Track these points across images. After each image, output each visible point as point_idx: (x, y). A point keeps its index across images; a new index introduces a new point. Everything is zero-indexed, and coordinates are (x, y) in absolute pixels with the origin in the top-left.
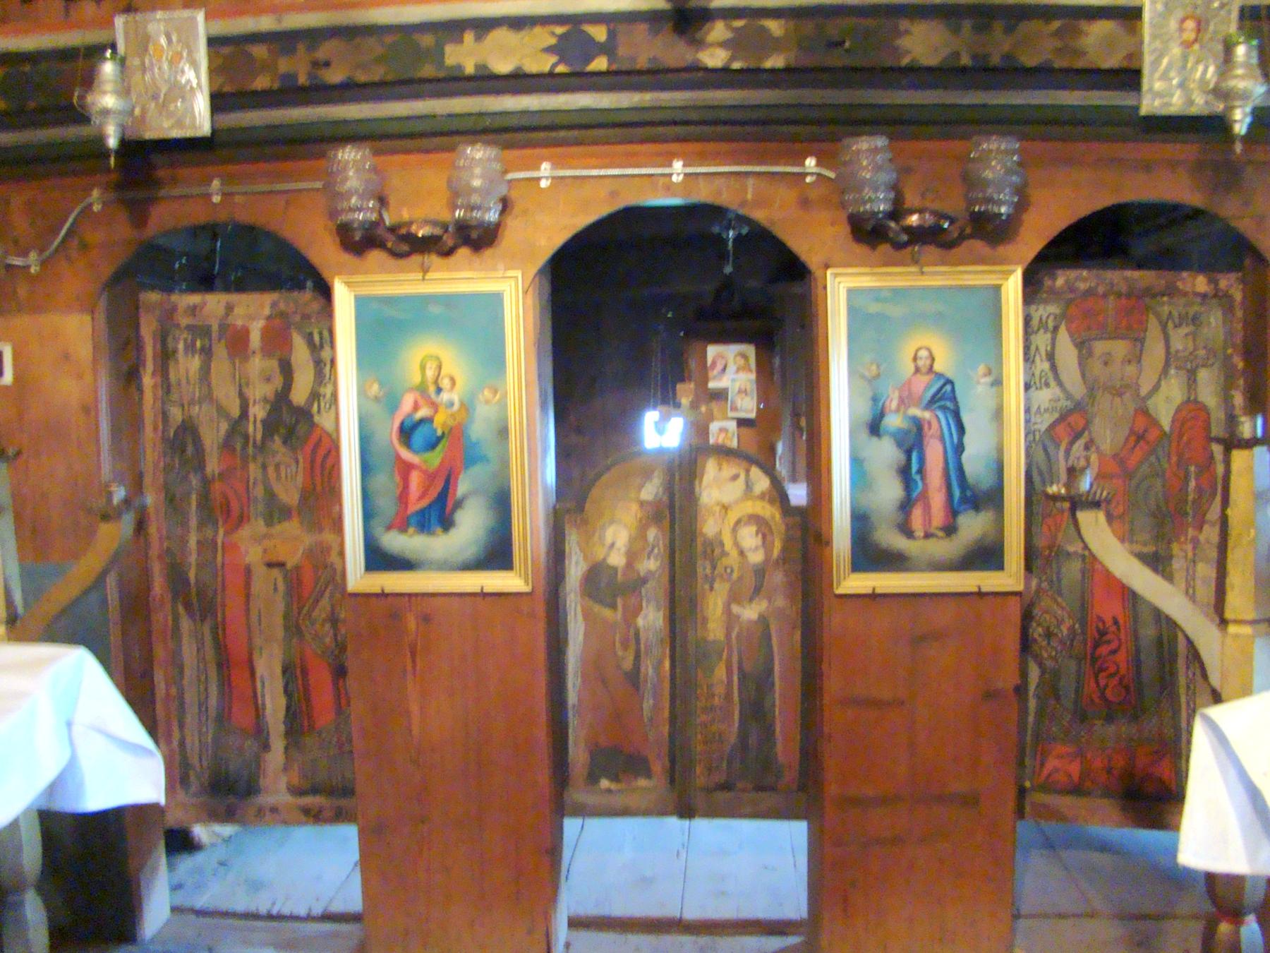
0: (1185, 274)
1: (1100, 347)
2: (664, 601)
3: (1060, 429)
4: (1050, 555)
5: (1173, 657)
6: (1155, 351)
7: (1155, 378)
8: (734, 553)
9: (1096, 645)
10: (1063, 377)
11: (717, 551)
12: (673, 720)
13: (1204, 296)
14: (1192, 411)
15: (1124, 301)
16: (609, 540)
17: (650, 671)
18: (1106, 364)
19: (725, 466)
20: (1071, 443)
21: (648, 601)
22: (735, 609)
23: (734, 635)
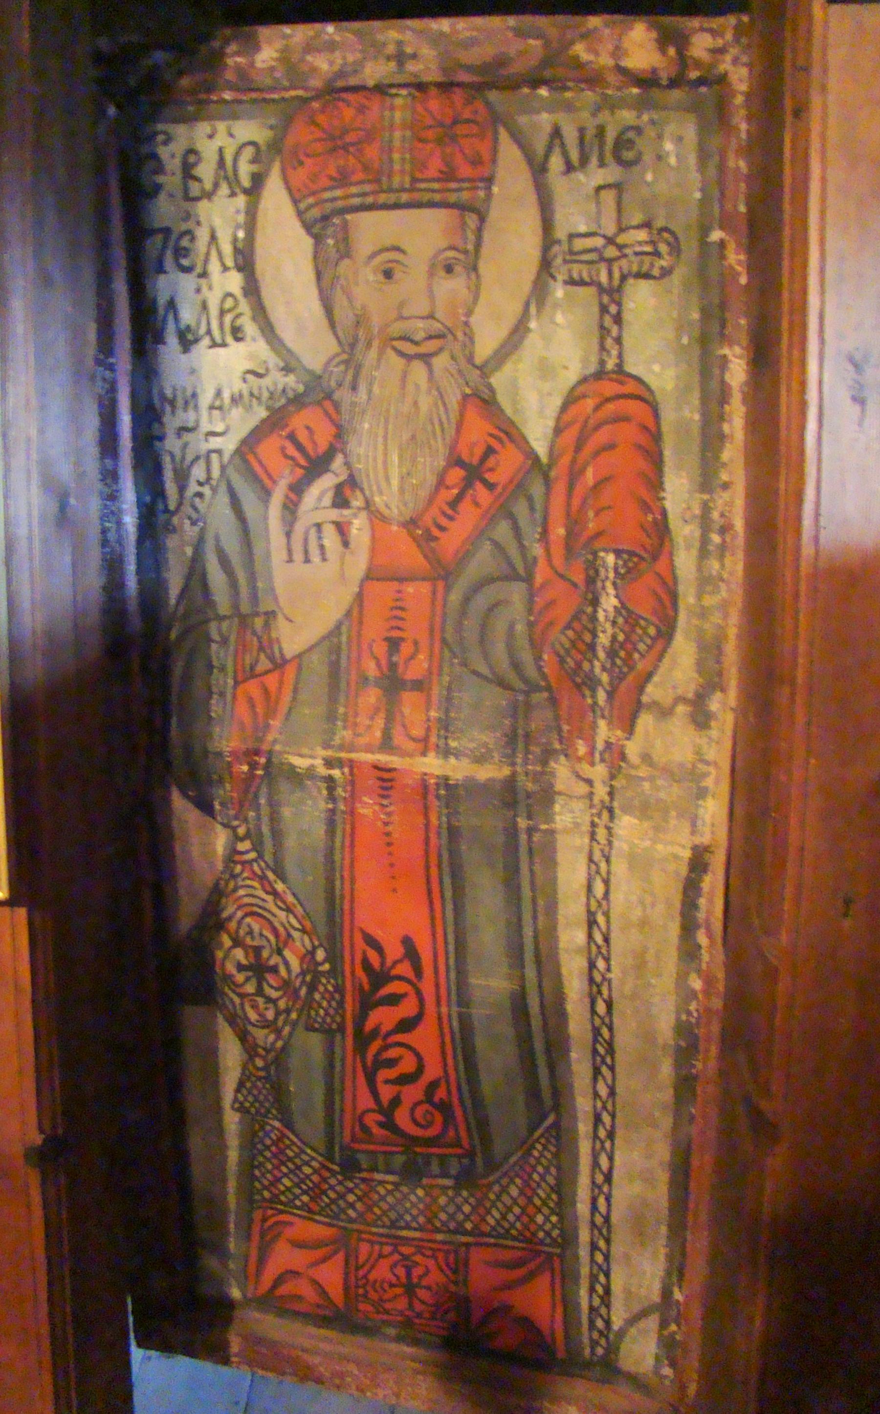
0: (594, 21)
1: (372, 229)
3: (270, 450)
4: (251, 775)
5: (557, 1045)
6: (514, 237)
7: (513, 309)
9: (366, 1005)
10: (278, 312)
13: (647, 81)
14: (611, 398)
15: (435, 104)
18: (388, 274)
20: (297, 489)
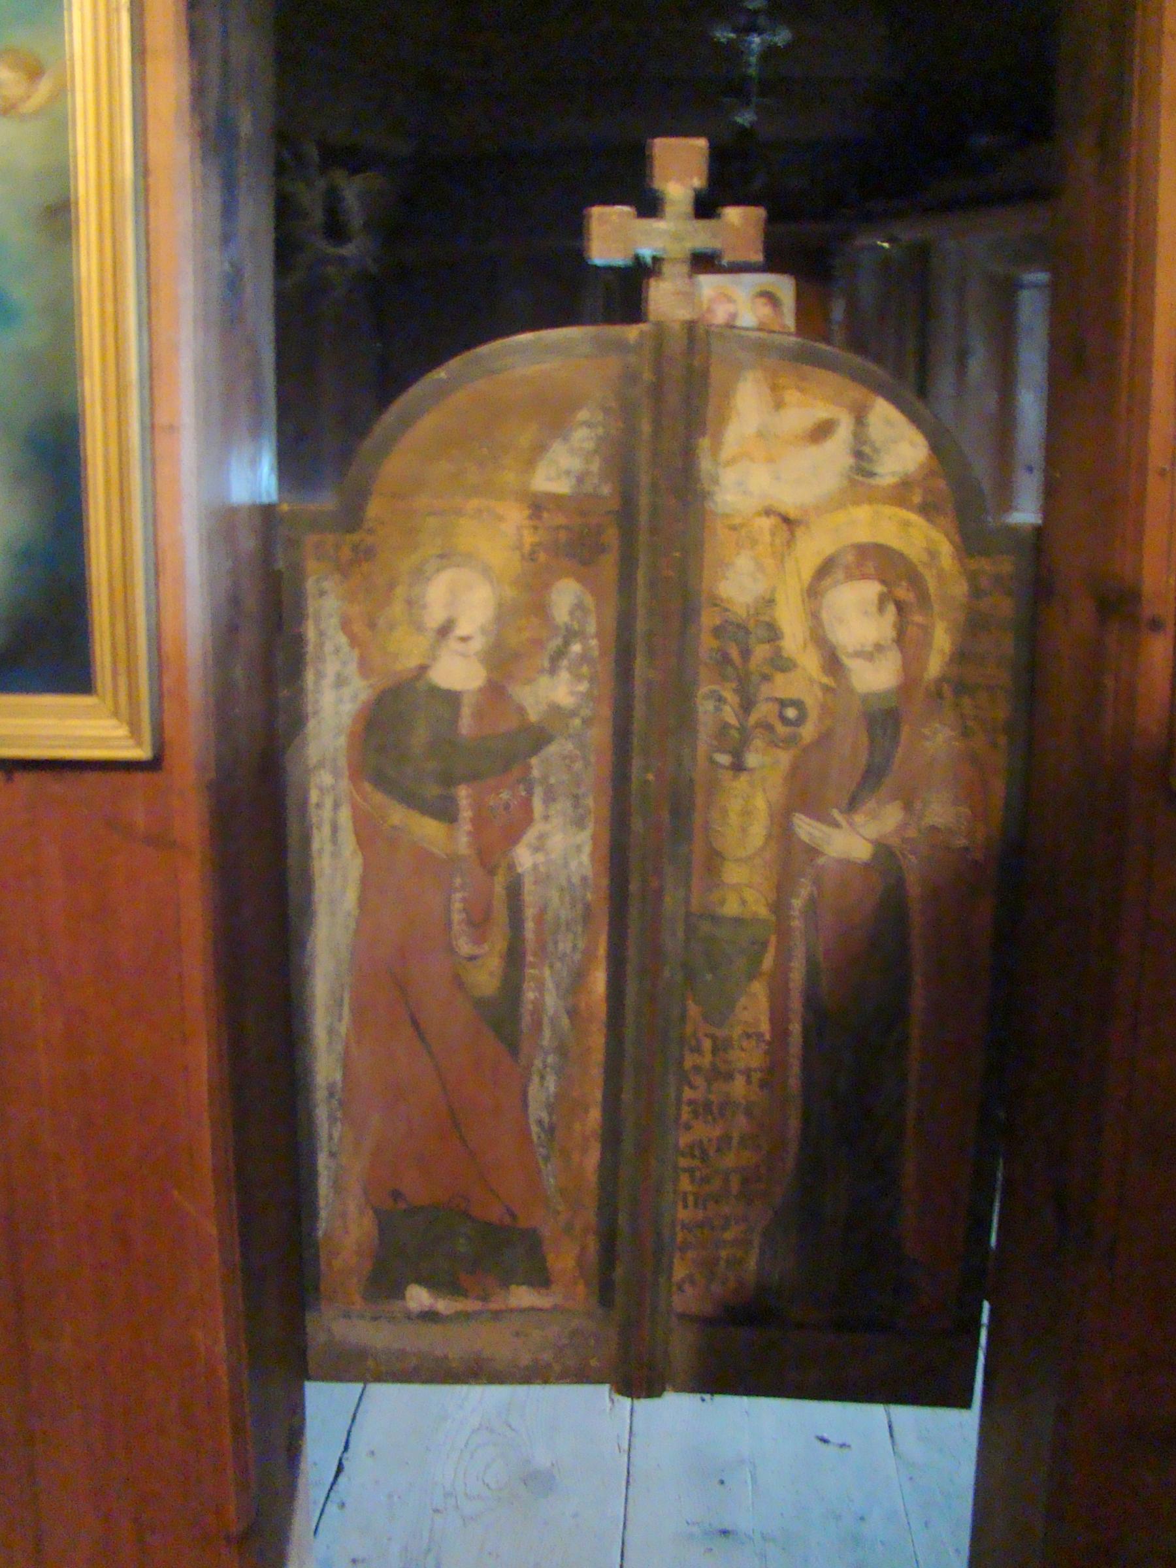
2: (595, 803)
8: (810, 662)
11: (761, 652)
12: (611, 1136)
16: (435, 616)
17: (552, 1002)
19: (792, 396)
21: (550, 797)
22: (806, 828)
23: (797, 903)
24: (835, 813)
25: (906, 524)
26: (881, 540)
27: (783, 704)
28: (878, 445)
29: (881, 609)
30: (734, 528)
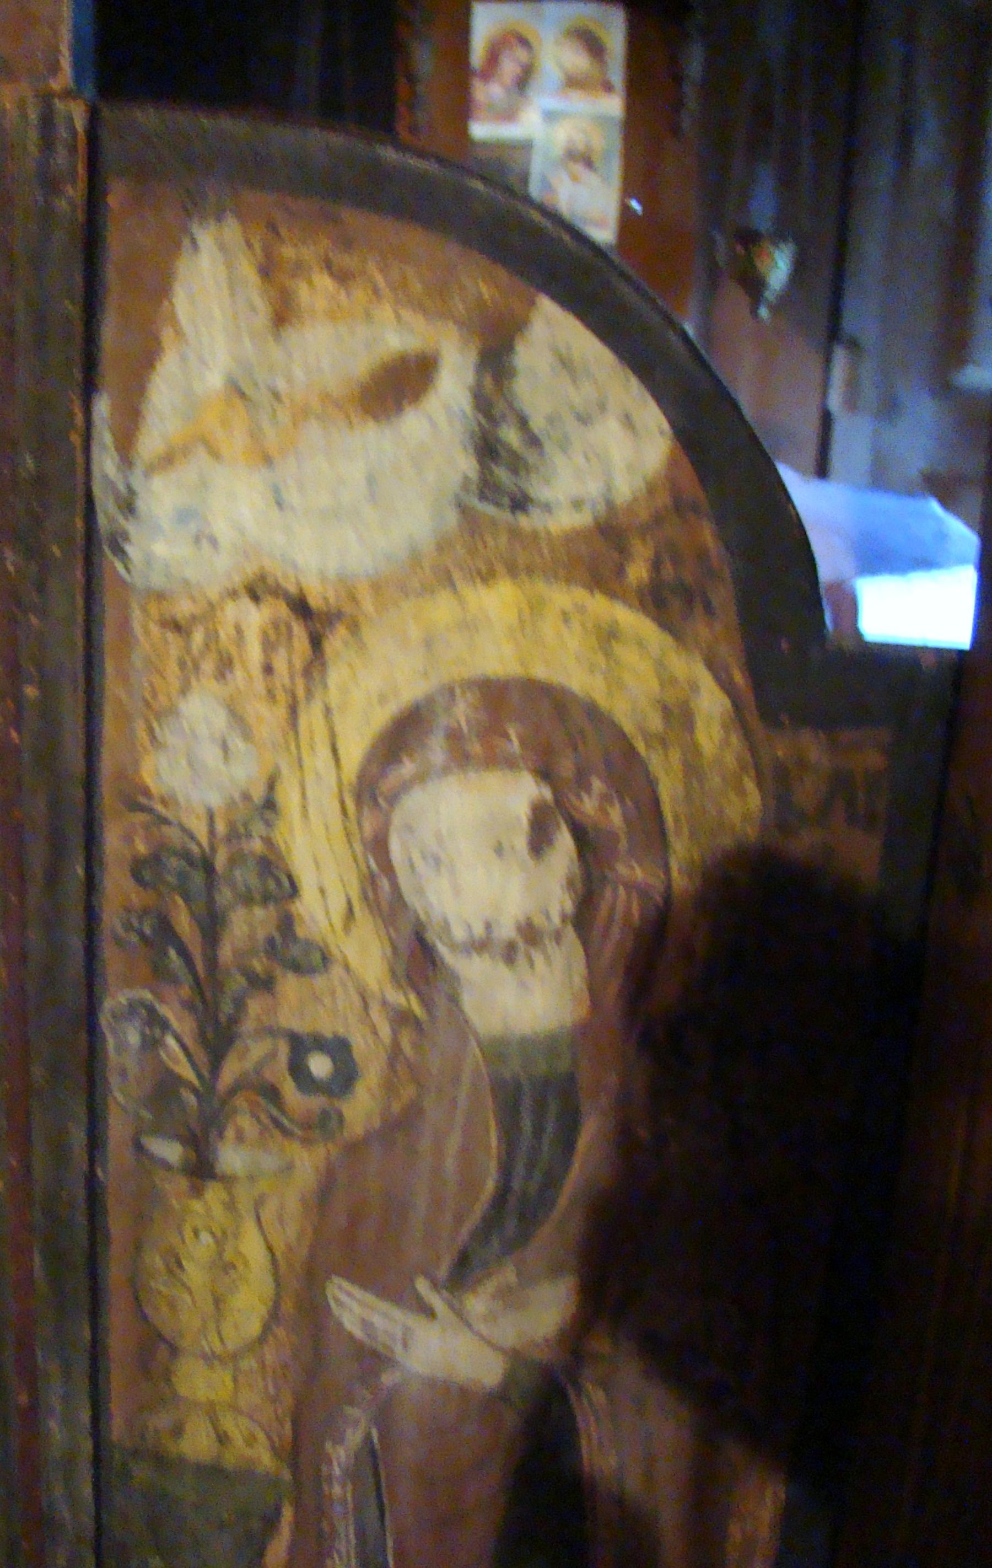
8: (365, 955)
11: (246, 926)
19: (316, 291)
22: (354, 1308)
23: (340, 1455)
24: (422, 1285)
25: (608, 636)
26: (540, 672)
27: (300, 1046)
28: (537, 423)
29: (539, 840)
30: (177, 627)
